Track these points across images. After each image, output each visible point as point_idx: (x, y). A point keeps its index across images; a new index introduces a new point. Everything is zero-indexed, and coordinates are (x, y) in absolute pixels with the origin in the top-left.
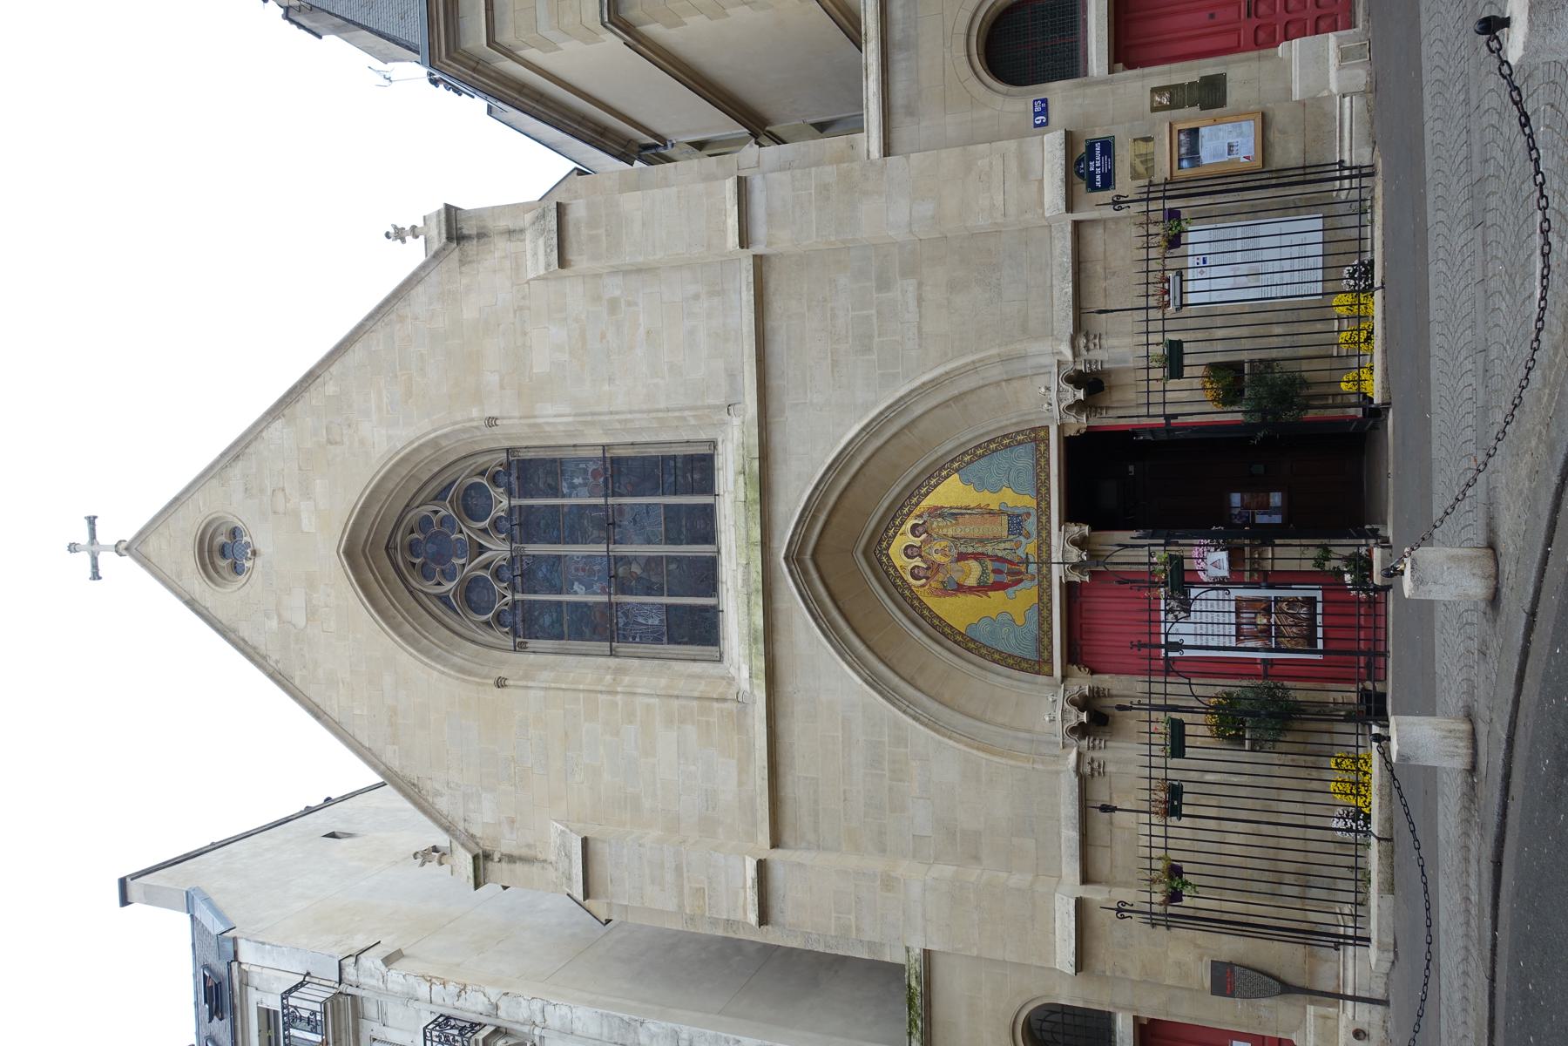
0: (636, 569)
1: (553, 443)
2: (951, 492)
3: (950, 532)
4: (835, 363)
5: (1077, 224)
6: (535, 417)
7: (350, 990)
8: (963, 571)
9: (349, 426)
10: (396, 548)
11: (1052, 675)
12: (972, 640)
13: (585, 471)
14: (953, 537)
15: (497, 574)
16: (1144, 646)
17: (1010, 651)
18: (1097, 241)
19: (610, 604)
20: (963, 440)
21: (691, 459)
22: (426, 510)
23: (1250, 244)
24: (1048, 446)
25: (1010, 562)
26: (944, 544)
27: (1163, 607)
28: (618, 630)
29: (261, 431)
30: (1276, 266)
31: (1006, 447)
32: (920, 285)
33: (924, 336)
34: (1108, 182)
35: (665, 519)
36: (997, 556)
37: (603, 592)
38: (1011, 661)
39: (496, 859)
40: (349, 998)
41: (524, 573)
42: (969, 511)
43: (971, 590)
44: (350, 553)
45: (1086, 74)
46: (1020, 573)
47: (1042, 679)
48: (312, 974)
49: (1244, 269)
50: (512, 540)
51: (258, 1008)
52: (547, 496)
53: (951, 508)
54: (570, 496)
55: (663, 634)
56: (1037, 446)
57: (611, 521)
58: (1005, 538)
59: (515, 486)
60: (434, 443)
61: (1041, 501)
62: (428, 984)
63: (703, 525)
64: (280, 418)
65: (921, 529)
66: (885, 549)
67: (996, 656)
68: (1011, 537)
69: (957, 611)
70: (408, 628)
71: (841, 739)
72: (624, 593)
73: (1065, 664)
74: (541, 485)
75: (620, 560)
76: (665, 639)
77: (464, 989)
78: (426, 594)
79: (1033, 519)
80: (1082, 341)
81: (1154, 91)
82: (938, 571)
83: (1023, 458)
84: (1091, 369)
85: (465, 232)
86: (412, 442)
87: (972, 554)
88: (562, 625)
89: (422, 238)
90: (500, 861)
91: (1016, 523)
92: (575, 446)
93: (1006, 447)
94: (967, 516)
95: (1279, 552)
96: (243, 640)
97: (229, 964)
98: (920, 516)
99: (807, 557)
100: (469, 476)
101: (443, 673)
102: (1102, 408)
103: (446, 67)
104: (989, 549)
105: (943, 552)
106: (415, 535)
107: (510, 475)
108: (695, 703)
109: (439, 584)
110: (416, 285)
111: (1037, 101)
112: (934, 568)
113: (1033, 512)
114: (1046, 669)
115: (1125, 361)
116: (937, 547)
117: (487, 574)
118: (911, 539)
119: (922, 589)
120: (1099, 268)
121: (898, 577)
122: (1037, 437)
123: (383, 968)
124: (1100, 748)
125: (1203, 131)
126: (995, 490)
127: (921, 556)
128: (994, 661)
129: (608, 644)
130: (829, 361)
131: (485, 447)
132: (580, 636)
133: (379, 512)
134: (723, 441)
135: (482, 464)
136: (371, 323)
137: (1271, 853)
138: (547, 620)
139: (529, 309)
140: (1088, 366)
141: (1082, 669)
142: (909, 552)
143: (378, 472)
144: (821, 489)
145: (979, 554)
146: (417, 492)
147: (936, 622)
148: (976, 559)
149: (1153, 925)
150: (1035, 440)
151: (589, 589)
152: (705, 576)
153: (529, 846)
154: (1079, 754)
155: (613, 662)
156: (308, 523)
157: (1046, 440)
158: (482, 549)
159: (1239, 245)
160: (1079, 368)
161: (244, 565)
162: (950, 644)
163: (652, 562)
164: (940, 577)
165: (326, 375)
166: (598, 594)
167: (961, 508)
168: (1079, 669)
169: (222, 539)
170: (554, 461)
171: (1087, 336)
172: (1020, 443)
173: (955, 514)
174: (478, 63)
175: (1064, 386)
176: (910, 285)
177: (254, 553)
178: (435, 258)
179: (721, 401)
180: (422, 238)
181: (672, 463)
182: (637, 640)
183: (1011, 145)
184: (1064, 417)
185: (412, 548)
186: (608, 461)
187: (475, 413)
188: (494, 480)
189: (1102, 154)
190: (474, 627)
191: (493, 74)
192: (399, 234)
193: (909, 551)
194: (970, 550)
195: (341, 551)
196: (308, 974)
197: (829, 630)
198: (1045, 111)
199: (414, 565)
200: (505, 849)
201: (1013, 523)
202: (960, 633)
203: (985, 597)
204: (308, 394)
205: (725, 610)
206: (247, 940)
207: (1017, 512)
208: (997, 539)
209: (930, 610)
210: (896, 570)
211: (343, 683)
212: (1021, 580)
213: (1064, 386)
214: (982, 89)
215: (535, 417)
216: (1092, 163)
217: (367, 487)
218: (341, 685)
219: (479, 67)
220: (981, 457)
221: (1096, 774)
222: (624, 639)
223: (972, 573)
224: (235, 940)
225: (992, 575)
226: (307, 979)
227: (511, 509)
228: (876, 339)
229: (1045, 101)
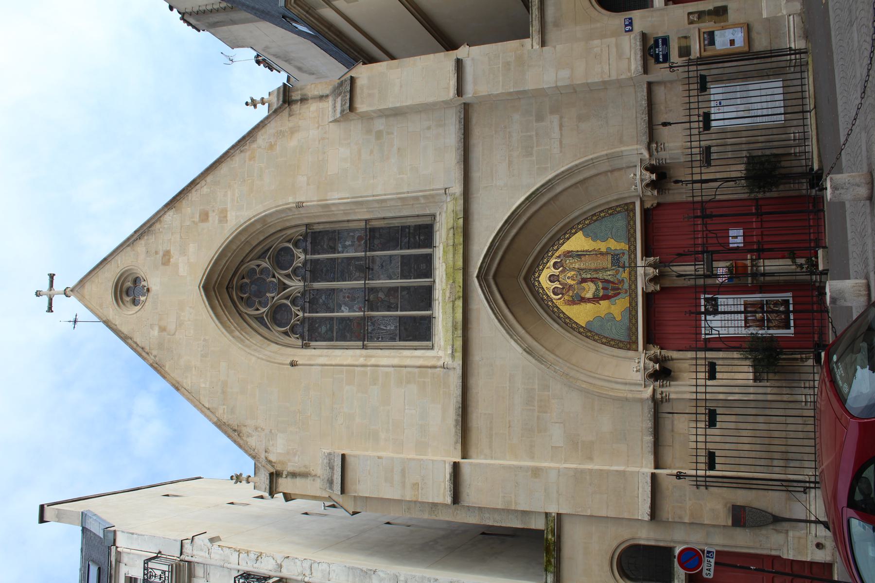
0: (381, 295)
1: (335, 219)
2: (578, 242)
3: (577, 266)
4: (510, 163)
5: (650, 85)
6: (327, 200)
7: (187, 559)
8: (584, 289)
9: (213, 211)
10: (233, 288)
11: (638, 351)
12: (590, 331)
13: (353, 237)
14: (578, 269)
15: (294, 302)
16: (693, 313)
17: (612, 336)
18: (660, 93)
19: (364, 318)
20: (585, 209)
22: (253, 265)
23: (744, 94)
24: (635, 214)
25: (613, 283)
26: (573, 273)
27: (703, 332)
28: (368, 333)
29: (160, 217)
30: (759, 106)
31: (611, 215)
32: (561, 118)
33: (563, 146)
34: (666, 58)
35: (401, 264)
36: (605, 279)
37: (360, 310)
38: (613, 343)
39: (284, 476)
40: (186, 563)
41: (311, 300)
42: (588, 253)
43: (589, 300)
45: (652, 6)
46: (618, 289)
47: (631, 353)
48: (162, 553)
49: (742, 107)
50: (305, 281)
51: (125, 576)
52: (329, 253)
53: (577, 251)
54: (343, 253)
55: (396, 335)
56: (628, 214)
57: (367, 266)
59: (309, 247)
60: (263, 220)
61: (631, 245)
62: (238, 553)
63: (425, 266)
64: (172, 208)
65: (559, 264)
66: (537, 278)
67: (604, 340)
68: (614, 267)
69: (581, 314)
70: (237, 333)
71: (508, 388)
72: (372, 310)
73: (645, 343)
74: (325, 247)
75: (373, 290)
76: (398, 338)
77: (261, 555)
78: (248, 315)
79: (626, 257)
80: (654, 145)
81: (689, 14)
82: (569, 290)
83: (620, 222)
84: (659, 164)
85: (294, 98)
86: (250, 219)
87: (590, 278)
88: (332, 332)
89: (267, 105)
90: (286, 477)
91: (616, 258)
92: (348, 221)
93: (611, 215)
94: (587, 256)
95: (767, 262)
96: (136, 343)
97: (109, 548)
99: (490, 278)
100: (281, 242)
101: (258, 358)
102: (665, 190)
103: (293, 8)
104: (600, 275)
105: (572, 278)
106: (246, 280)
107: (307, 241)
108: (417, 370)
110: (262, 128)
111: (626, 19)
114: (634, 347)
115: (678, 159)
116: (569, 275)
117: (288, 302)
119: (558, 301)
120: (662, 108)
121: (544, 294)
122: (628, 208)
123: (209, 544)
124: (667, 386)
125: (716, 33)
126: (604, 240)
127: (559, 281)
129: (362, 342)
130: (507, 161)
131: (293, 223)
132: (344, 339)
133: (225, 264)
134: (440, 214)
135: (290, 235)
136: (232, 151)
137: (766, 441)
138: (323, 329)
139: (328, 139)
140: (658, 161)
141: (655, 346)
142: (552, 279)
143: (228, 238)
144: (500, 235)
145: (592, 278)
146: (248, 253)
147: (568, 321)
148: (592, 281)
149: (698, 486)
150: (627, 210)
151: (351, 309)
152: (425, 297)
154: (654, 390)
155: (364, 352)
156: (183, 270)
157: (634, 210)
158: (286, 286)
159: (738, 95)
160: (652, 162)
161: (140, 300)
163: (393, 290)
164: (571, 293)
165: (203, 183)
167: (583, 251)
168: (654, 347)
169: (129, 284)
170: (334, 231)
171: (657, 143)
172: (619, 212)
173: (579, 255)
174: (310, 9)
175: (644, 172)
176: (555, 118)
177: (148, 290)
178: (275, 113)
179: (442, 186)
180: (267, 105)
181: (407, 230)
182: (380, 339)
183: (613, 40)
184: (644, 191)
185: (242, 288)
186: (368, 230)
187: (291, 200)
188: (296, 245)
189: (663, 45)
190: (277, 334)
191: (316, 16)
192: (254, 103)
193: (552, 278)
194: (589, 276)
195: (201, 286)
196: (160, 552)
197: (502, 319)
198: (631, 24)
199: (242, 298)
200: (290, 468)
201: (614, 259)
202: (582, 327)
203: (597, 304)
204: (190, 194)
205: (437, 318)
206: (123, 532)
207: (617, 252)
208: (605, 269)
209: (564, 314)
211: (195, 368)
212: (619, 294)
213: (644, 172)
214: (596, 13)
215: (327, 200)
216: (657, 49)
217: (220, 247)
218: (194, 369)
219: (310, 11)
220: (595, 221)
221: (664, 400)
222: (371, 339)
223: (590, 290)
224: (115, 532)
225: (602, 291)
226: (159, 555)
227: (306, 261)
228: (535, 149)
229: (630, 19)
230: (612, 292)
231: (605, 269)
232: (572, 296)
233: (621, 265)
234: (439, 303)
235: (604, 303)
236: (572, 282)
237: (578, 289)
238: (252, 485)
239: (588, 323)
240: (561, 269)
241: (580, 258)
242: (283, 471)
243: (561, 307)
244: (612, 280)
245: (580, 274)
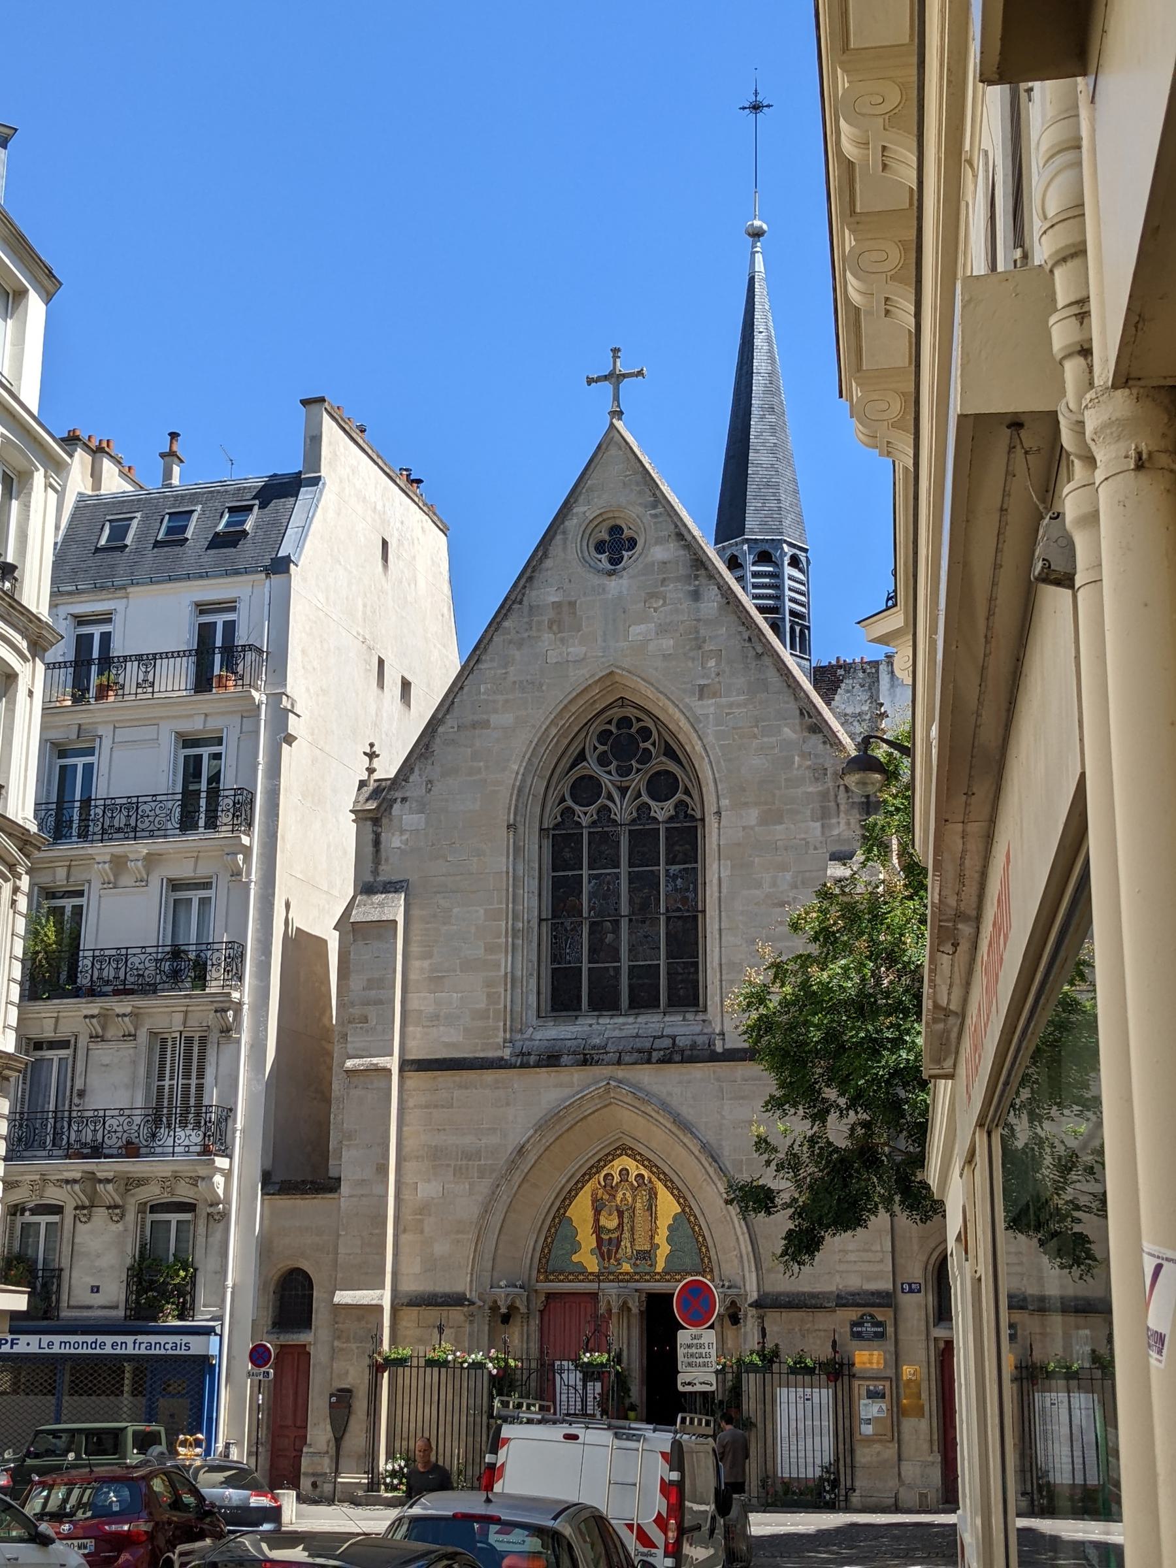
0: (610, 937)
3: (638, 1205)
8: (610, 1215)
13: (687, 890)
23: (817, 1431)
26: (630, 1200)
39: (375, 828)
46: (609, 1259)
49: (801, 1426)
50: (633, 821)
53: (656, 1206)
63: (643, 1000)
65: (641, 1181)
67: (549, 1240)
74: (677, 848)
75: (616, 923)
79: (648, 1269)
82: (610, 1195)
91: (647, 1256)
101: (517, 773)
104: (626, 1235)
105: (624, 1198)
112: (611, 1190)
113: (652, 1269)
116: (628, 1194)
118: (633, 1173)
126: (669, 1240)
128: (546, 1238)
138: (567, 855)
142: (624, 1172)
148: (619, 1225)
152: (605, 1003)
153: (387, 860)
162: (558, 1203)
164: (606, 1197)
166: (589, 902)
173: (651, 1208)
181: (692, 970)
188: (681, 804)
189: (875, 1332)
193: (624, 1172)
194: (626, 1220)
198: (911, 1291)
202: (565, 1212)
209: (581, 1188)
211: (506, 673)
212: (604, 1260)
220: (693, 1229)
222: (554, 927)
223: (610, 1222)
225: (607, 1237)
229: (919, 1291)
232: (602, 1199)
233: (638, 1262)
234: (591, 1025)
236: (618, 1199)
238: (365, 776)
240: (635, 1184)
242: (381, 826)
243: (589, 1184)
244: (620, 1250)
245: (627, 1209)
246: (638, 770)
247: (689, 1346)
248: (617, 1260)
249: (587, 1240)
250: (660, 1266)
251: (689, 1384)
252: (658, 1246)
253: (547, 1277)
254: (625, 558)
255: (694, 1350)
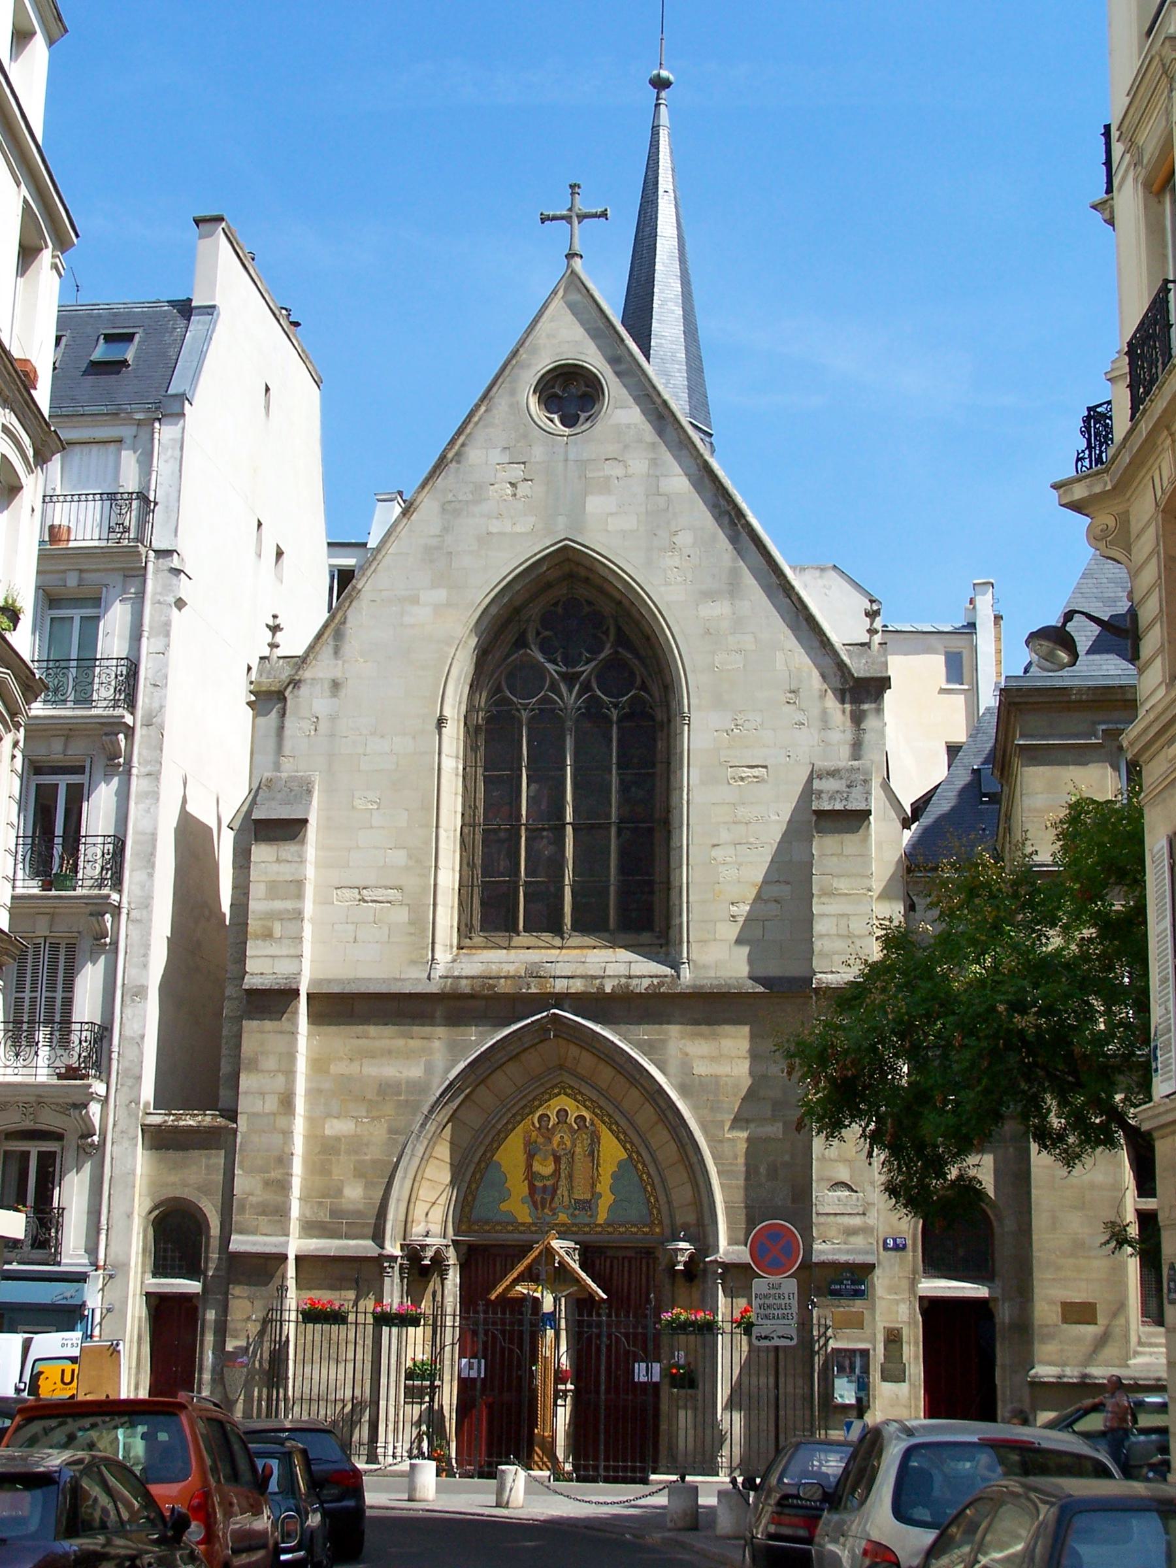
2: (612, 1151)
3: (578, 1150)
8: (545, 1159)
21: (650, 909)
25: (553, 1199)
26: (569, 1144)
36: (557, 1189)
43: (529, 1166)
44: (566, 547)
46: (543, 1208)
53: (599, 1151)
58: (572, 1196)
67: (474, 1186)
68: (573, 1201)
79: (587, 1220)
93: (649, 1201)
98: (592, 1124)
104: (563, 1182)
105: (562, 1142)
109: (538, 634)
112: (547, 1132)
116: (566, 1137)
142: (562, 1113)
147: (502, 1135)
148: (555, 1171)
164: (541, 1140)
167: (598, 1159)
173: (593, 1155)
193: (562, 1113)
194: (563, 1167)
207: (593, 1206)
208: (571, 1190)
210: (547, 1101)
212: (537, 1209)
220: (641, 1178)
223: (545, 1168)
230: (539, 1199)
231: (571, 1190)
232: (536, 1142)
235: (524, 1189)
237: (547, 1150)
238: (266, 652)
239: (499, 1165)
241: (589, 1155)
244: (556, 1199)
245: (566, 1154)
246: (588, 662)
247: (765, 1296)
248: (552, 1210)
249: (518, 1187)
250: (602, 1218)
251: (766, 1338)
252: (600, 1196)
253: (469, 1227)
254: (582, 419)
255: (771, 1301)
